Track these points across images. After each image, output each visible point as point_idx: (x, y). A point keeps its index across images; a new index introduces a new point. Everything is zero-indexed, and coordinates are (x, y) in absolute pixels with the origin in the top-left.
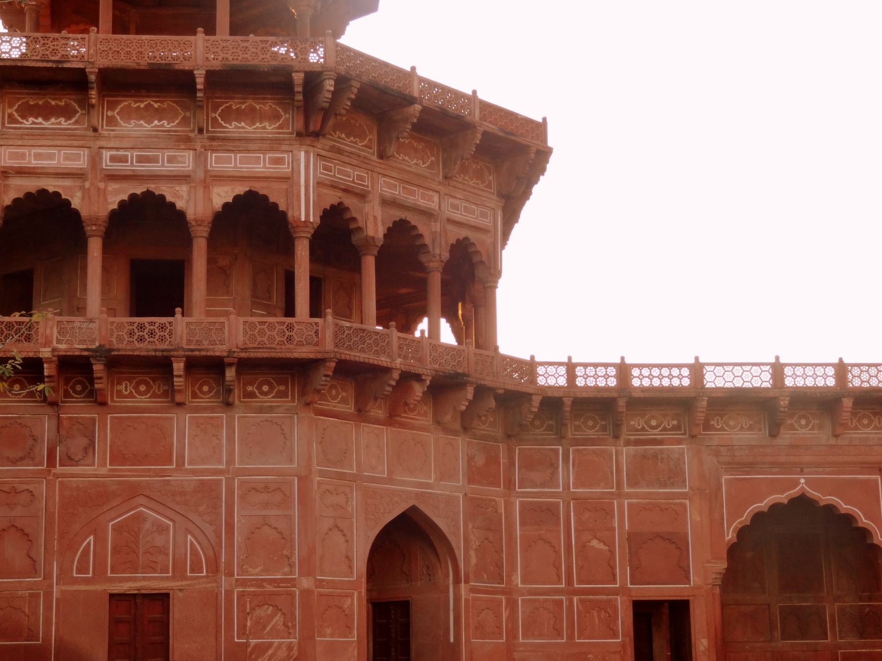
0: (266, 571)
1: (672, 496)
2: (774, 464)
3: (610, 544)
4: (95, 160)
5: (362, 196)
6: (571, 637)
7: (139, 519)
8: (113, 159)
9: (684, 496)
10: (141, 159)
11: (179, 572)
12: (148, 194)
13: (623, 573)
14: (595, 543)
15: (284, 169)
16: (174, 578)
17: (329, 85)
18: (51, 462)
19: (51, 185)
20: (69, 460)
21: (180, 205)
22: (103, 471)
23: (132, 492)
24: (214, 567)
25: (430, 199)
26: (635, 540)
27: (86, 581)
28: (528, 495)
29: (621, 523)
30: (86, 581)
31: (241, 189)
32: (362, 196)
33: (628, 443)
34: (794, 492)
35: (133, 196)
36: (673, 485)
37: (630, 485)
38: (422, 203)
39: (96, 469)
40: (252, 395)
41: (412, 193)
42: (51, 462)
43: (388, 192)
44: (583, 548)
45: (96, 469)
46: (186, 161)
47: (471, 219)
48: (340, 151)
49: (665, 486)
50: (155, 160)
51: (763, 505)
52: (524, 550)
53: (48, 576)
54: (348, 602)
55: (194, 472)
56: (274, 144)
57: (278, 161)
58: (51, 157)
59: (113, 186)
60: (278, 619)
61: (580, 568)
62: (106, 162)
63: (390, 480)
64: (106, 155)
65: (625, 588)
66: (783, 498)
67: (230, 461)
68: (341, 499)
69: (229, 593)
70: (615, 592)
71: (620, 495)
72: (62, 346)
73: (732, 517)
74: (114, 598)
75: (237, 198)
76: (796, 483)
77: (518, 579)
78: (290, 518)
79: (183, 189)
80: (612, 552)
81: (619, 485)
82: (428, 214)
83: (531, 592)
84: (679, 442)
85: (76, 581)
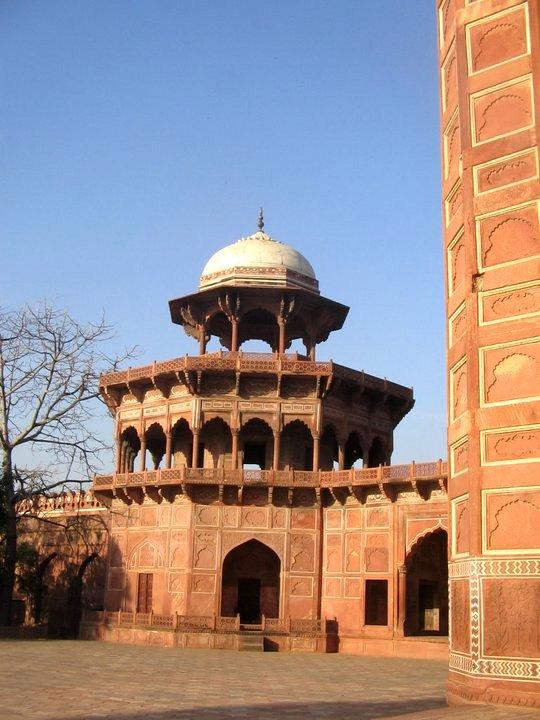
2: (428, 513)
5: (228, 412)
19: (132, 424)
25: (272, 406)
26: (369, 553)
29: (363, 544)
32: (228, 412)
33: (367, 506)
34: (436, 527)
36: (384, 525)
38: (266, 409)
47: (299, 411)
49: (381, 525)
51: (423, 534)
56: (187, 399)
62: (145, 414)
64: (145, 411)
66: (431, 530)
77: (324, 569)
82: (270, 413)
84: (386, 504)
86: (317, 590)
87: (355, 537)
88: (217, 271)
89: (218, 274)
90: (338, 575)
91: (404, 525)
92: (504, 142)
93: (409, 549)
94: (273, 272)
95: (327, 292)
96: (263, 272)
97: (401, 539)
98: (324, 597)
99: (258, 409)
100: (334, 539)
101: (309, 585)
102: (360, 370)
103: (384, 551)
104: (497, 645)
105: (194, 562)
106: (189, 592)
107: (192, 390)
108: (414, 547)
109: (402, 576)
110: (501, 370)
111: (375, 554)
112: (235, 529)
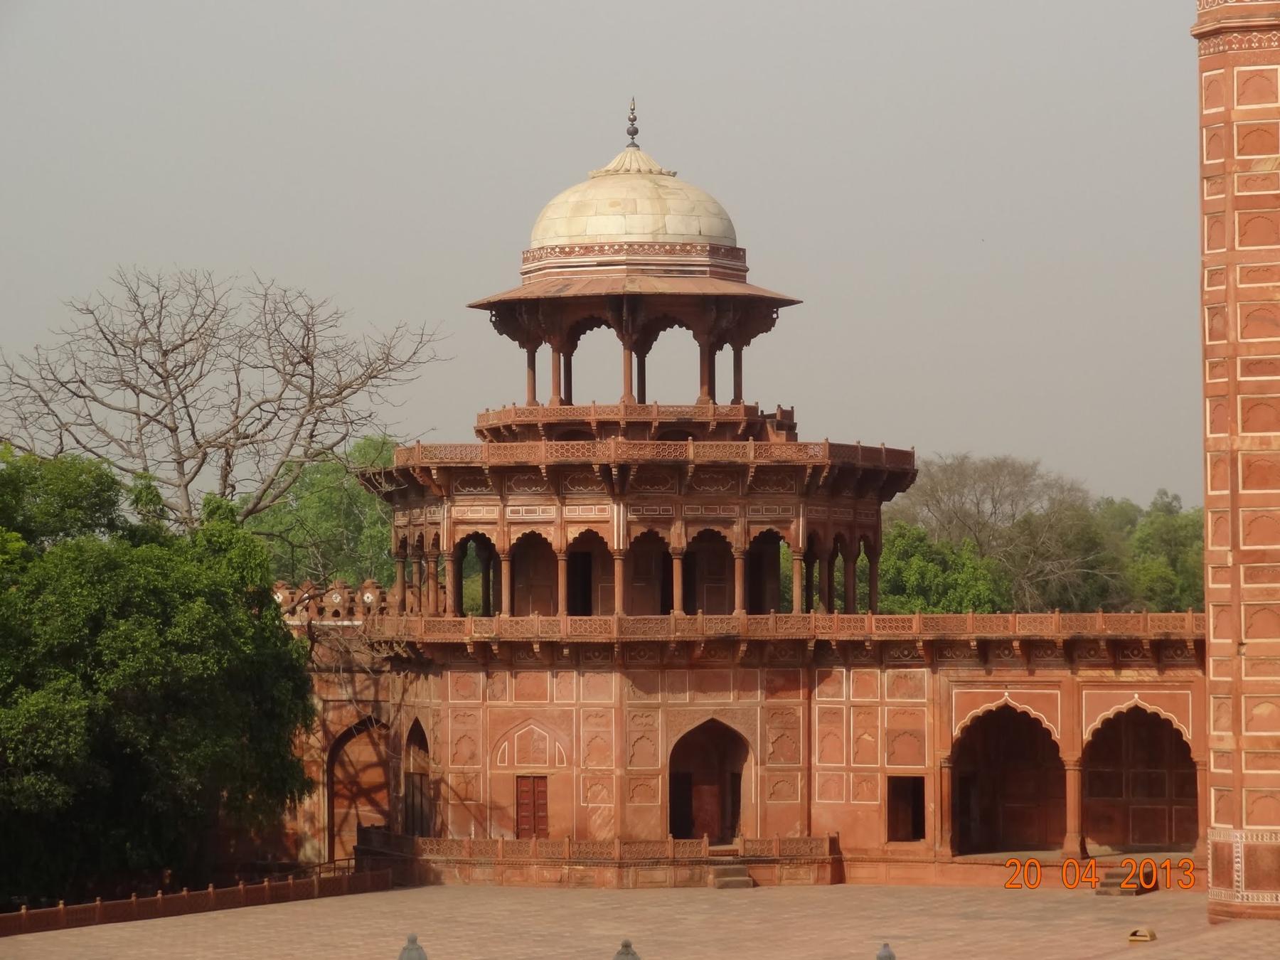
0: (598, 764)
1: (915, 705)
3: (875, 736)
4: (503, 514)
6: (848, 800)
7: (531, 732)
8: (513, 512)
9: (923, 705)
10: (527, 512)
11: (553, 764)
12: (533, 533)
13: (882, 757)
14: (866, 736)
15: (606, 516)
16: (550, 768)
17: (614, 471)
18: (484, 699)
20: (493, 697)
21: (550, 539)
22: (511, 704)
23: (527, 717)
24: (570, 762)
26: (893, 736)
27: (505, 768)
28: (823, 703)
29: (883, 721)
30: (505, 768)
31: (583, 528)
34: (1000, 702)
35: (524, 534)
36: (916, 697)
37: (889, 696)
38: (723, 515)
39: (507, 702)
40: (589, 658)
41: (715, 510)
42: (484, 699)
43: (690, 514)
44: (858, 740)
45: (507, 702)
46: (552, 512)
48: (646, 498)
49: (911, 697)
50: (534, 512)
51: (979, 711)
52: (821, 741)
53: (484, 765)
54: (653, 782)
55: (558, 705)
57: (603, 510)
58: (478, 512)
59: (513, 528)
60: (605, 792)
61: (856, 753)
63: (691, 704)
65: (885, 767)
66: (992, 706)
67: (578, 698)
68: (649, 720)
69: (578, 777)
70: (876, 770)
71: (882, 704)
72: (477, 635)
73: (958, 721)
74: (520, 778)
75: (581, 534)
76: (1002, 695)
77: (815, 760)
78: (609, 732)
79: (551, 529)
80: (876, 742)
81: (882, 697)
83: (824, 769)
85: (499, 768)
86: (805, 791)
87: (866, 711)
88: (586, 241)
89: (587, 250)
90: (841, 769)
91: (950, 697)
92: (1264, 553)
93: (956, 732)
94: (689, 252)
95: (761, 278)
96: (672, 252)
97: (945, 718)
98: (816, 799)
99: (713, 515)
100: (832, 715)
101: (794, 785)
102: (854, 443)
103: (918, 736)
104: (1253, 882)
105: (627, 758)
106: (622, 802)
107: (617, 490)
108: (966, 730)
109: (946, 771)
110: (1257, 711)
111: (904, 738)
112: (685, 705)
